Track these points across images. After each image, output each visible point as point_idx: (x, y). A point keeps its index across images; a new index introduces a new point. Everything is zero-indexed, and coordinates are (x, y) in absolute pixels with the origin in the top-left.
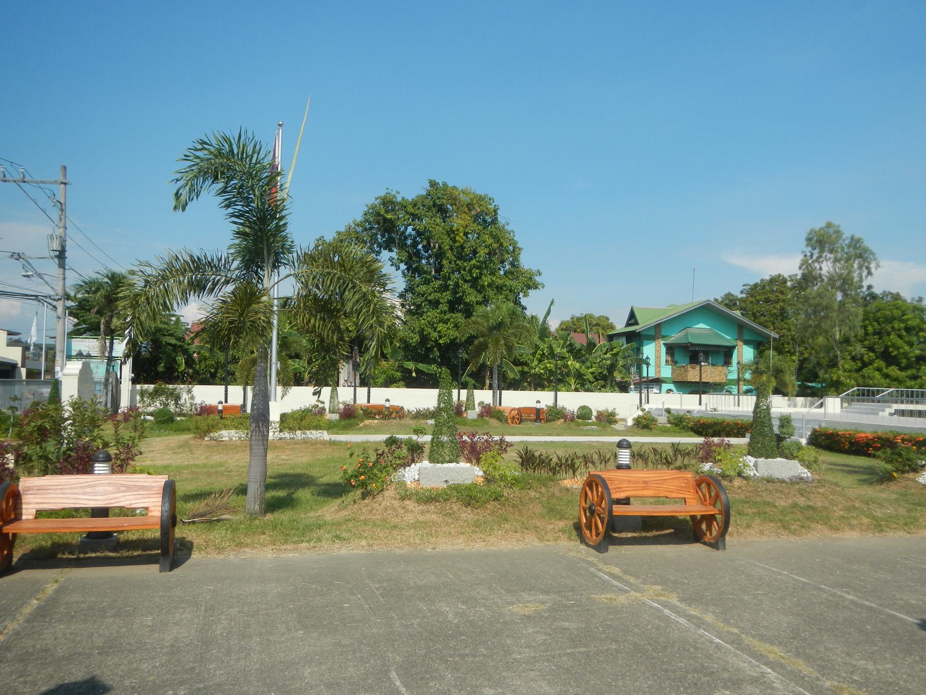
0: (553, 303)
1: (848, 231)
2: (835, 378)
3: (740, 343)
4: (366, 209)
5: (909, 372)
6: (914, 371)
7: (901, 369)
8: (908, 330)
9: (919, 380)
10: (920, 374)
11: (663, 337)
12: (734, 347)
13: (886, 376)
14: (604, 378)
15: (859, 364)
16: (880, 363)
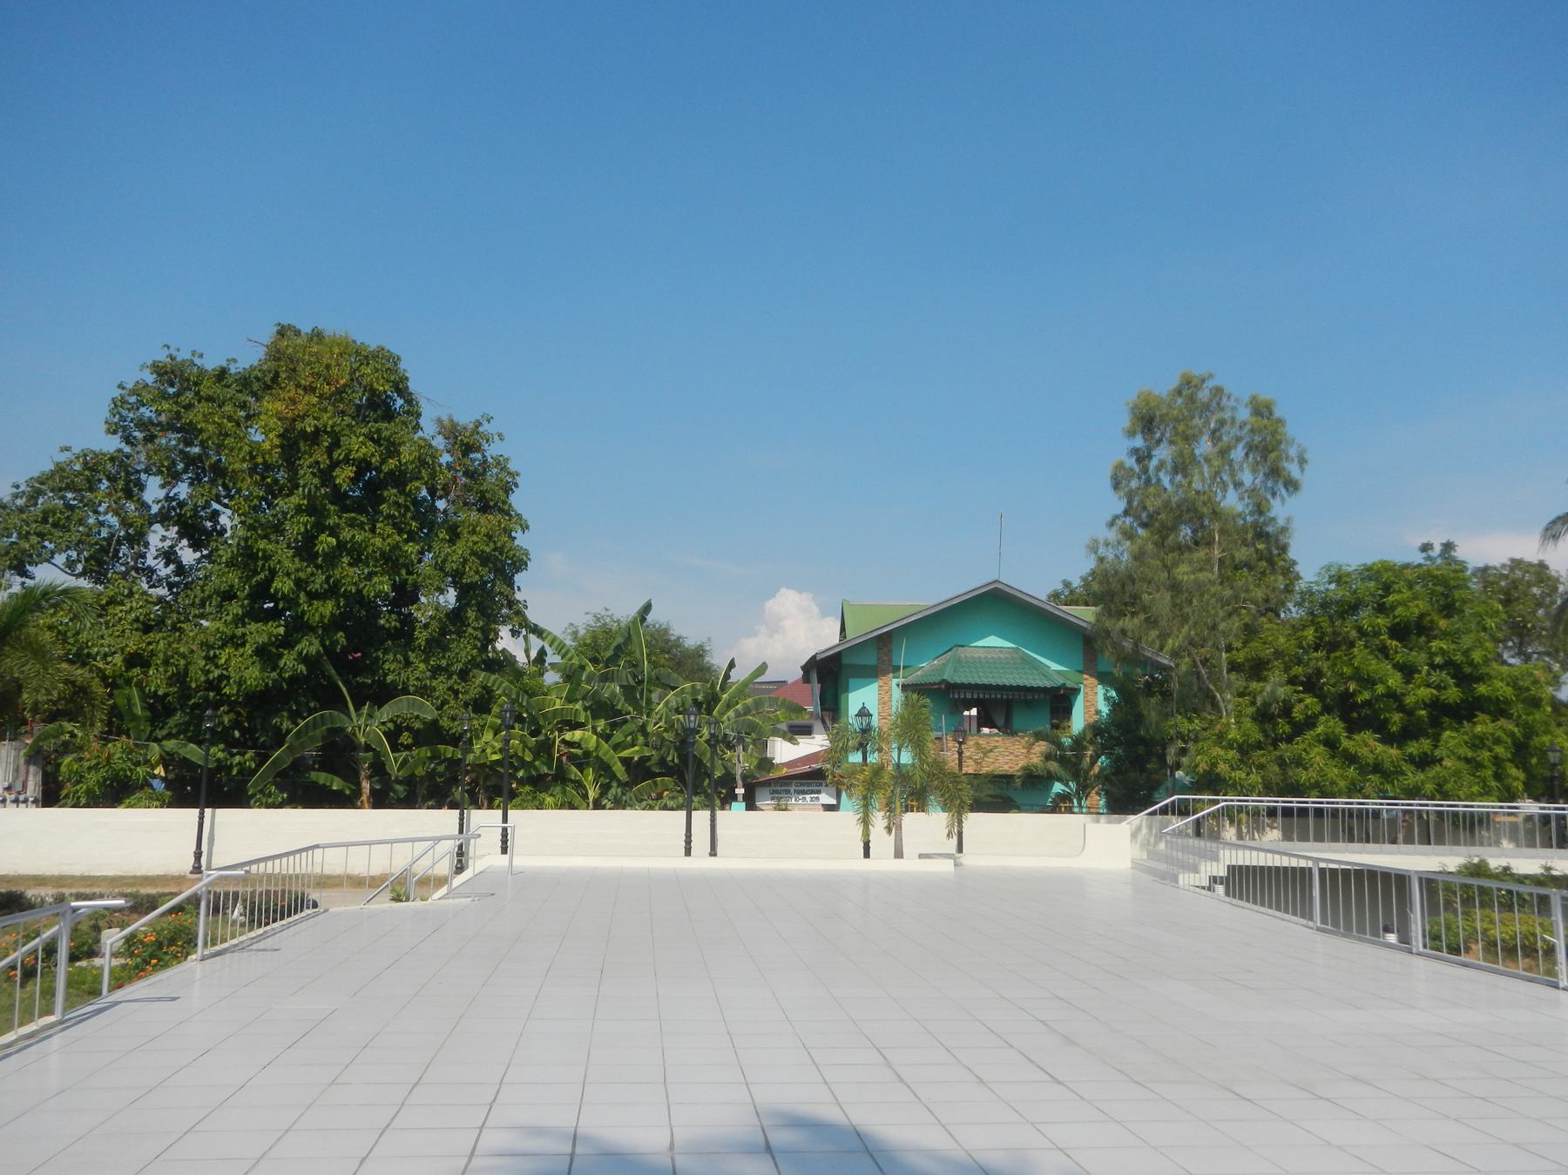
0: (563, 596)
1: (1240, 384)
2: (1203, 767)
3: (1093, 681)
4: (117, 393)
5: (1413, 748)
6: (1425, 744)
7: (1388, 739)
8: (1400, 632)
9: (1438, 768)
10: (1437, 753)
11: (896, 669)
12: (1076, 691)
13: (1350, 759)
14: (677, 772)
15: (1284, 727)
16: (1330, 724)
